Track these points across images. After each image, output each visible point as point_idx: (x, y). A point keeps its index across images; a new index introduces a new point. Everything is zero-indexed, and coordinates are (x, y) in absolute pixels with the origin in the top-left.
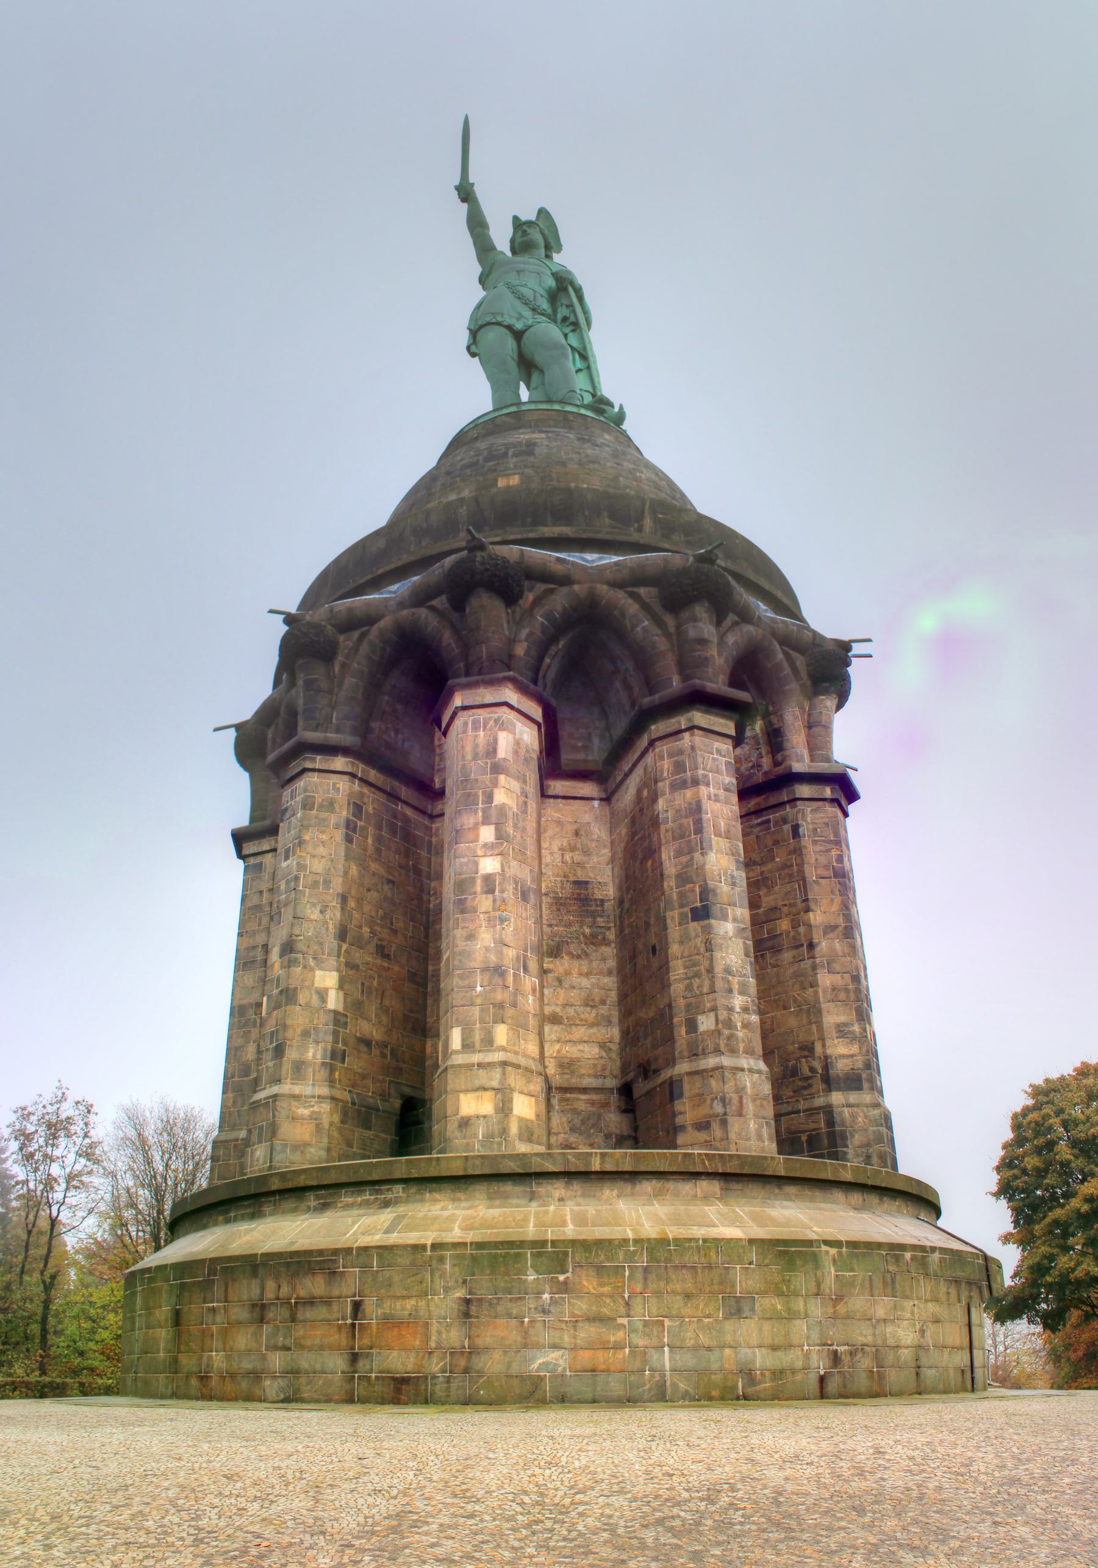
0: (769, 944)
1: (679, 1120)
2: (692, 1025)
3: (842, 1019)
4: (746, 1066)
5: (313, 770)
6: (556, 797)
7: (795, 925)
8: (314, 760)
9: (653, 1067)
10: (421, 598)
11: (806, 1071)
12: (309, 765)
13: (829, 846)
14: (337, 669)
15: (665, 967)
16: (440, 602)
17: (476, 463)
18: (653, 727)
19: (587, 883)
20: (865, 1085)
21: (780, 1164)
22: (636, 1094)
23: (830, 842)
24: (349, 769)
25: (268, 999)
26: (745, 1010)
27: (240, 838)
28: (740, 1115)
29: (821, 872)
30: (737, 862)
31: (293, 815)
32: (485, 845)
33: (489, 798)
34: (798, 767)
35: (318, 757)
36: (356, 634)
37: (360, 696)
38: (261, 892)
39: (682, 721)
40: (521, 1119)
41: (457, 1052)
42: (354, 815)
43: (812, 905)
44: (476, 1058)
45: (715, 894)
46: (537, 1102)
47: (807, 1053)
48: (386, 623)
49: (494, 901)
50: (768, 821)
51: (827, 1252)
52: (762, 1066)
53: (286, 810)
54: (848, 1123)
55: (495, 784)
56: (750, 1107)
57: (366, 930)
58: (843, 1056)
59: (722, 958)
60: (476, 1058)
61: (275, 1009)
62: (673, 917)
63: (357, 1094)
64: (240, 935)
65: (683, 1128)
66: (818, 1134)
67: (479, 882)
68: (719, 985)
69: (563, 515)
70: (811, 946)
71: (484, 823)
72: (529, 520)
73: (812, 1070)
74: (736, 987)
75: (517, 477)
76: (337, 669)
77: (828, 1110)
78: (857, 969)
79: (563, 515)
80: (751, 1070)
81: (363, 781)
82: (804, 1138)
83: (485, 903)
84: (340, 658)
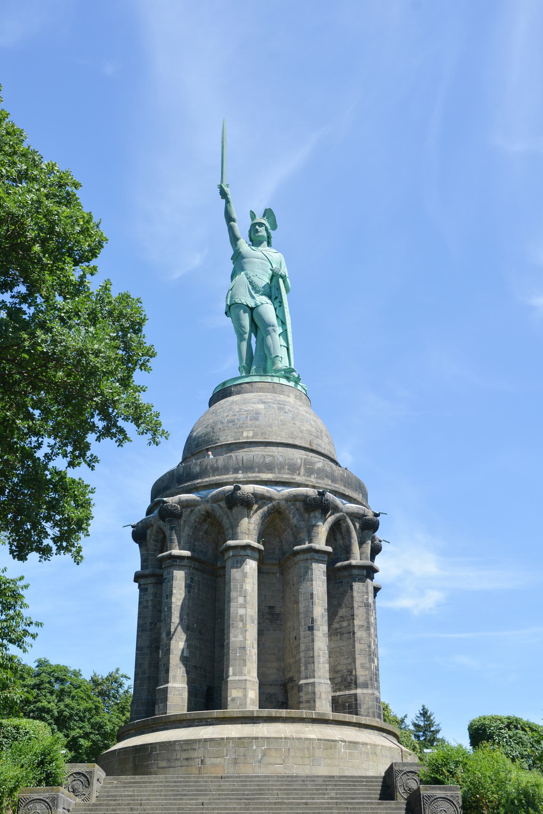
0: (339, 630)
1: (301, 700)
2: (306, 668)
3: (363, 661)
4: (323, 682)
5: (176, 565)
6: (263, 573)
7: (349, 625)
8: (177, 561)
9: (294, 679)
10: (216, 499)
11: (349, 679)
12: (175, 564)
13: (363, 594)
14: (182, 522)
15: (298, 646)
16: (223, 504)
17: (233, 421)
18: (299, 556)
19: (273, 607)
20: (369, 686)
21: (331, 715)
22: (288, 687)
23: (364, 592)
24: (189, 565)
25: (162, 651)
26: (324, 663)
27: (138, 578)
28: (320, 698)
29: (360, 604)
30: (325, 609)
31: (169, 582)
32: (241, 604)
33: (242, 587)
34: (354, 562)
35: (178, 560)
36: (189, 510)
37: (191, 534)
38: (147, 601)
39: (308, 556)
40: (251, 699)
41: (231, 676)
42: (191, 582)
43: (355, 617)
44: (237, 678)
45: (316, 622)
46: (256, 692)
47: (350, 673)
48: (202, 508)
49: (243, 624)
50: (342, 582)
51: (341, 744)
52: (329, 682)
53: (166, 579)
54: (362, 701)
55: (244, 581)
56: (324, 696)
57: (195, 625)
58: (362, 675)
59: (317, 644)
60: (237, 678)
61: (165, 655)
62: (302, 629)
63: (193, 686)
64: (139, 618)
65: (302, 702)
66: (352, 704)
67: (238, 617)
68: (316, 654)
69: (269, 468)
70: (354, 633)
71: (240, 596)
72: (257, 469)
73: (351, 680)
74: (321, 654)
75: (251, 432)
76: (182, 522)
77: (355, 695)
78: (370, 643)
79: (269, 468)
80: (324, 683)
81: (195, 568)
82: (347, 705)
83: (241, 625)
84: (183, 518)
